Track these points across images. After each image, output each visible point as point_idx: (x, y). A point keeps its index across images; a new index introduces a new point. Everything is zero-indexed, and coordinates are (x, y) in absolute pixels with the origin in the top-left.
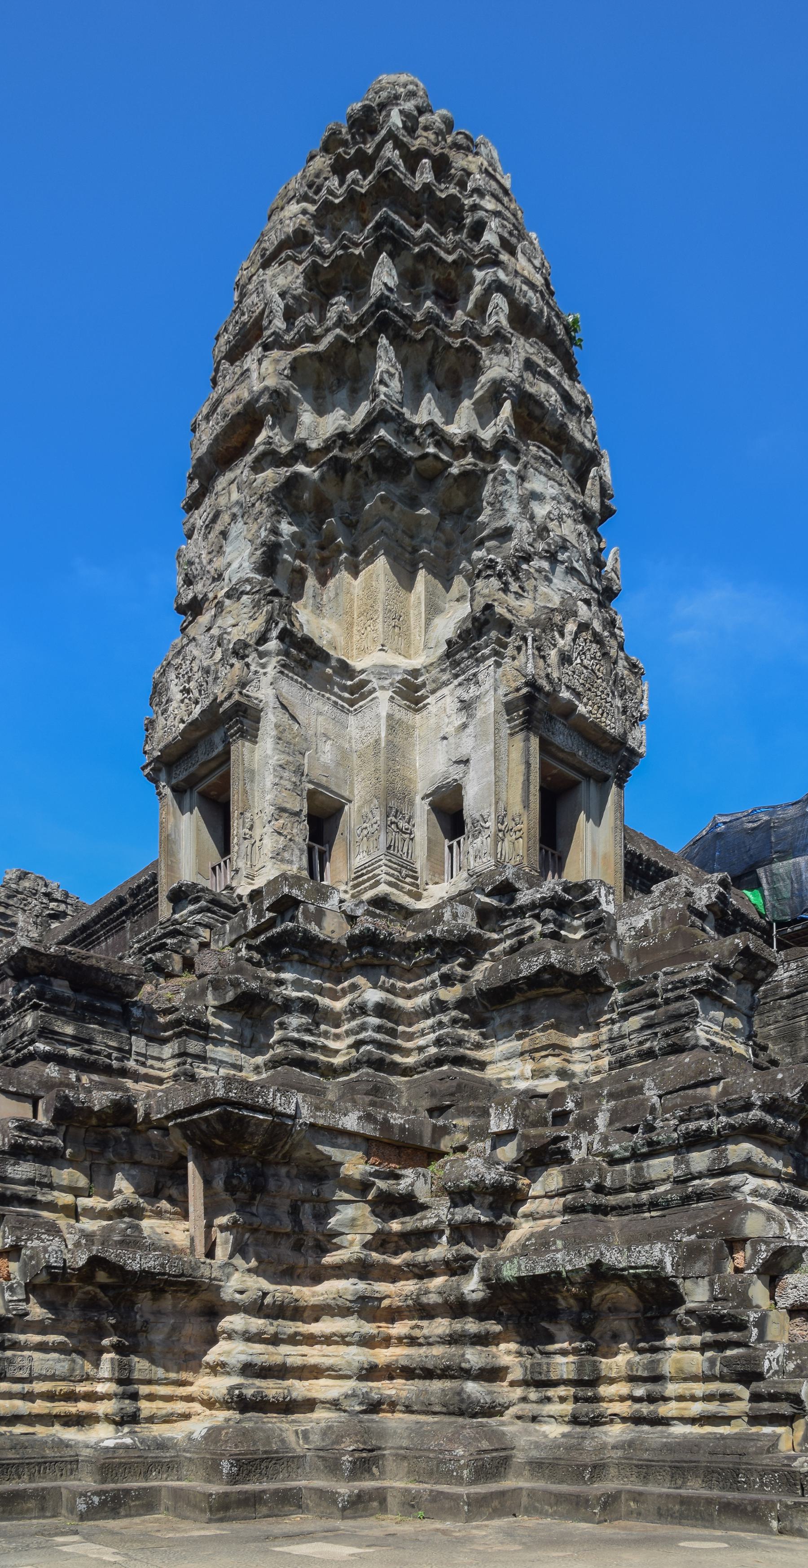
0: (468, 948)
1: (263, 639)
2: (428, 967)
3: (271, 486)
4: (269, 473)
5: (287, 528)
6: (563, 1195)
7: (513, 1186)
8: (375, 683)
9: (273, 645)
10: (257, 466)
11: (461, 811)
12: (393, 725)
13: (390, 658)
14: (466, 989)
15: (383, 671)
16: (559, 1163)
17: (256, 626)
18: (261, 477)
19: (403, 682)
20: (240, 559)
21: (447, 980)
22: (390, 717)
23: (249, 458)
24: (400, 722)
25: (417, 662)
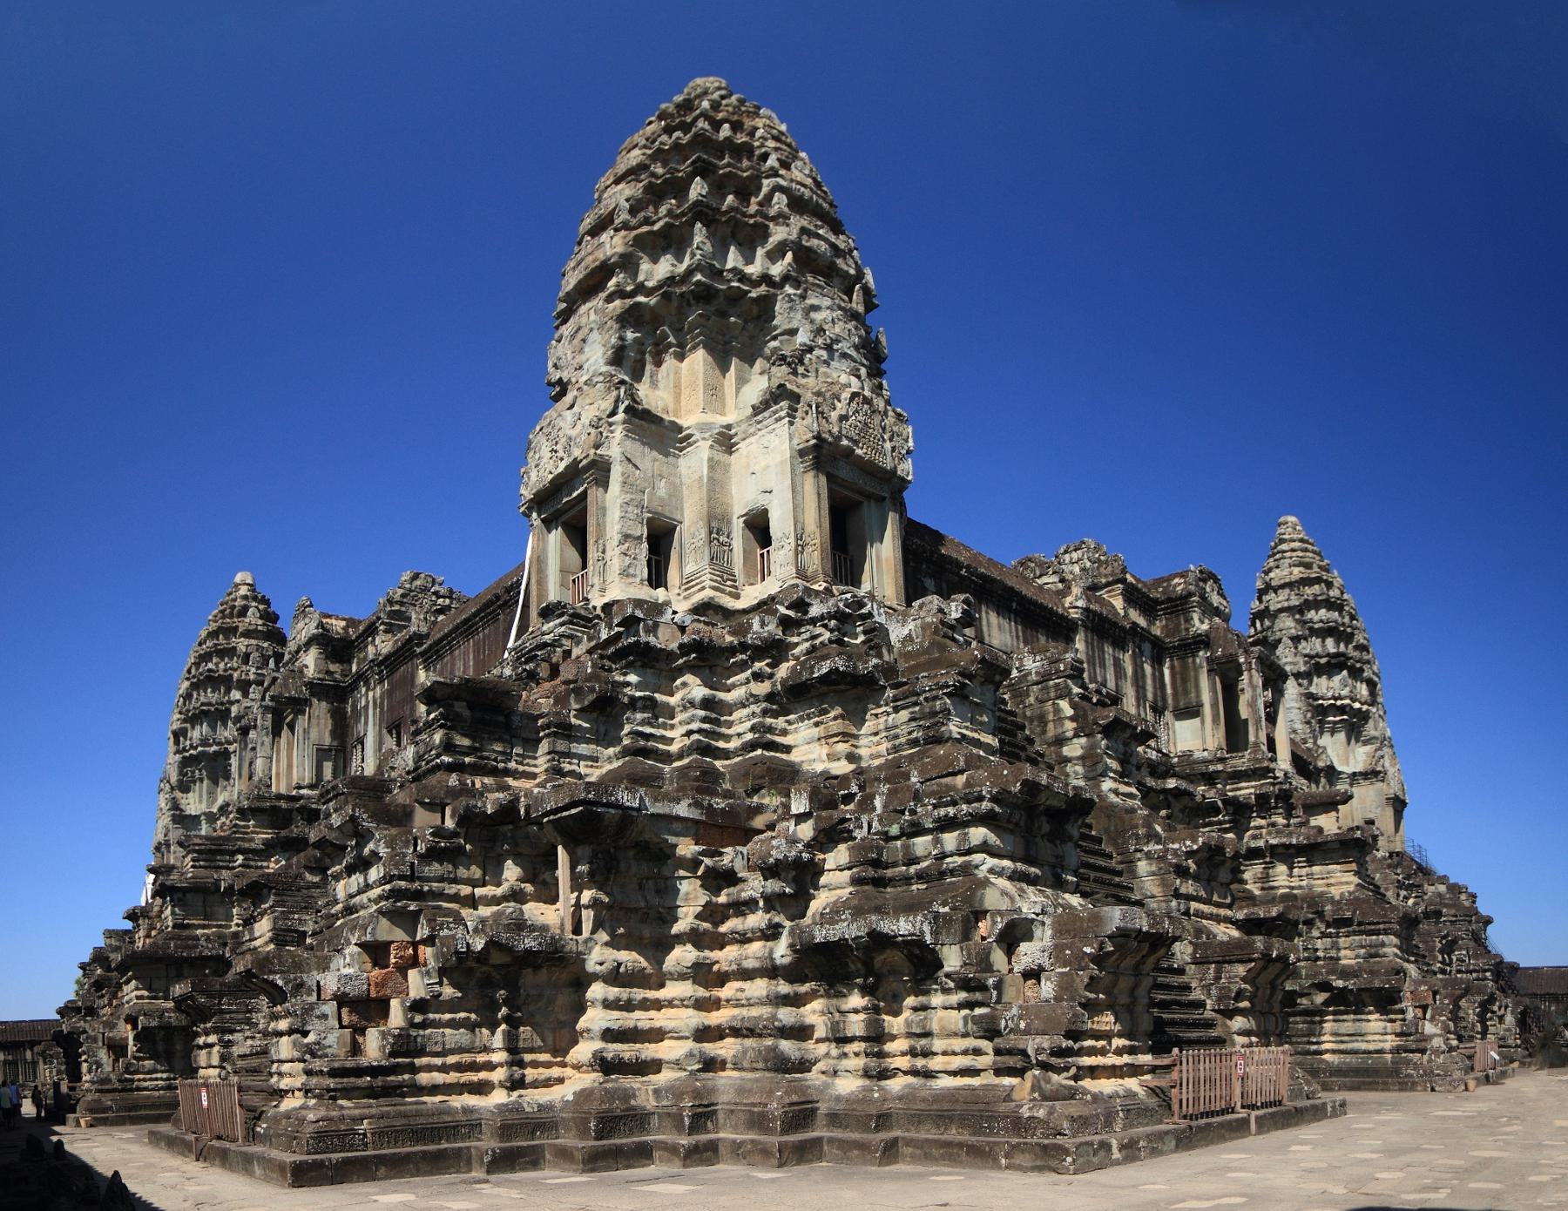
0: (774, 650)
1: (613, 413)
2: (743, 666)
3: (619, 311)
4: (618, 302)
5: (630, 335)
6: (849, 868)
7: (812, 859)
8: (697, 436)
9: (620, 416)
10: (609, 299)
11: (768, 528)
12: (713, 465)
13: (710, 418)
14: (774, 685)
15: (704, 427)
16: (845, 840)
17: (607, 405)
18: (611, 306)
19: (720, 434)
20: (596, 356)
21: (758, 677)
22: (710, 460)
23: (603, 295)
24: (718, 462)
25: (730, 418)
